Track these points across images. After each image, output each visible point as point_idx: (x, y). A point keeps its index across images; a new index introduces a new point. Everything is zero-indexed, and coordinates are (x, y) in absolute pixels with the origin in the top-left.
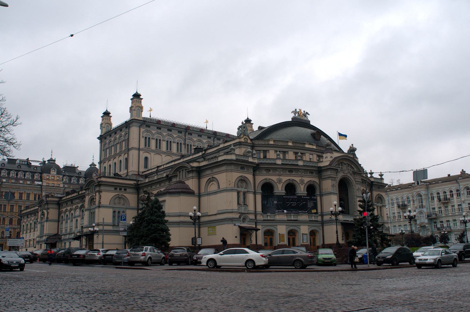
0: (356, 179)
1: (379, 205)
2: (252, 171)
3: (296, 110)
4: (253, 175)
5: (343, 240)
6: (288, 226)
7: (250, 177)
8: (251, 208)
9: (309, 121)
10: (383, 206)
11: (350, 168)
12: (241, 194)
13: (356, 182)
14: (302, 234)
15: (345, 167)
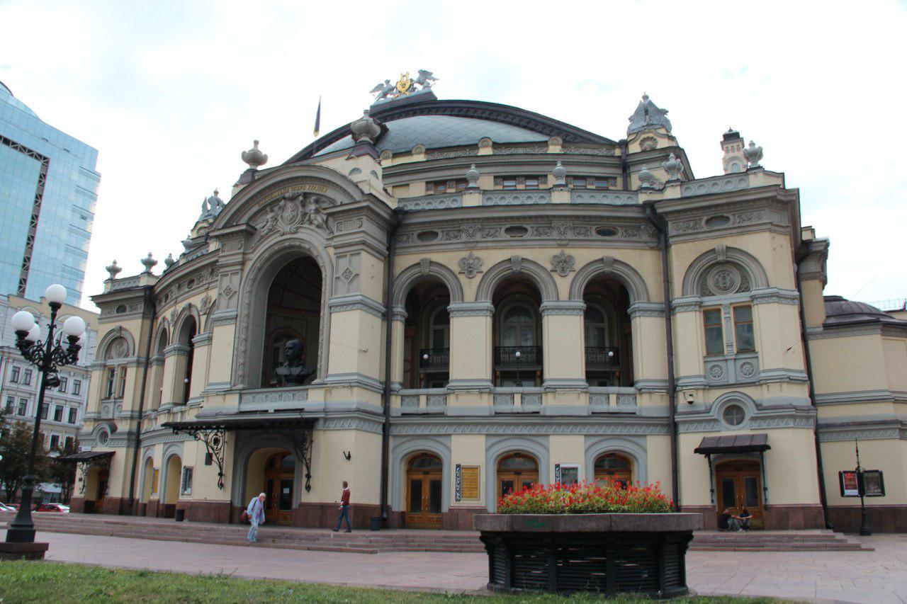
0: (335, 240)
1: (725, 300)
2: (141, 308)
3: (388, 82)
4: (143, 318)
5: (221, 485)
6: (166, 446)
7: (134, 325)
8: (128, 404)
9: (430, 93)
10: (753, 298)
11: (313, 207)
12: (118, 372)
13: (338, 251)
14: (185, 467)
15: (289, 210)
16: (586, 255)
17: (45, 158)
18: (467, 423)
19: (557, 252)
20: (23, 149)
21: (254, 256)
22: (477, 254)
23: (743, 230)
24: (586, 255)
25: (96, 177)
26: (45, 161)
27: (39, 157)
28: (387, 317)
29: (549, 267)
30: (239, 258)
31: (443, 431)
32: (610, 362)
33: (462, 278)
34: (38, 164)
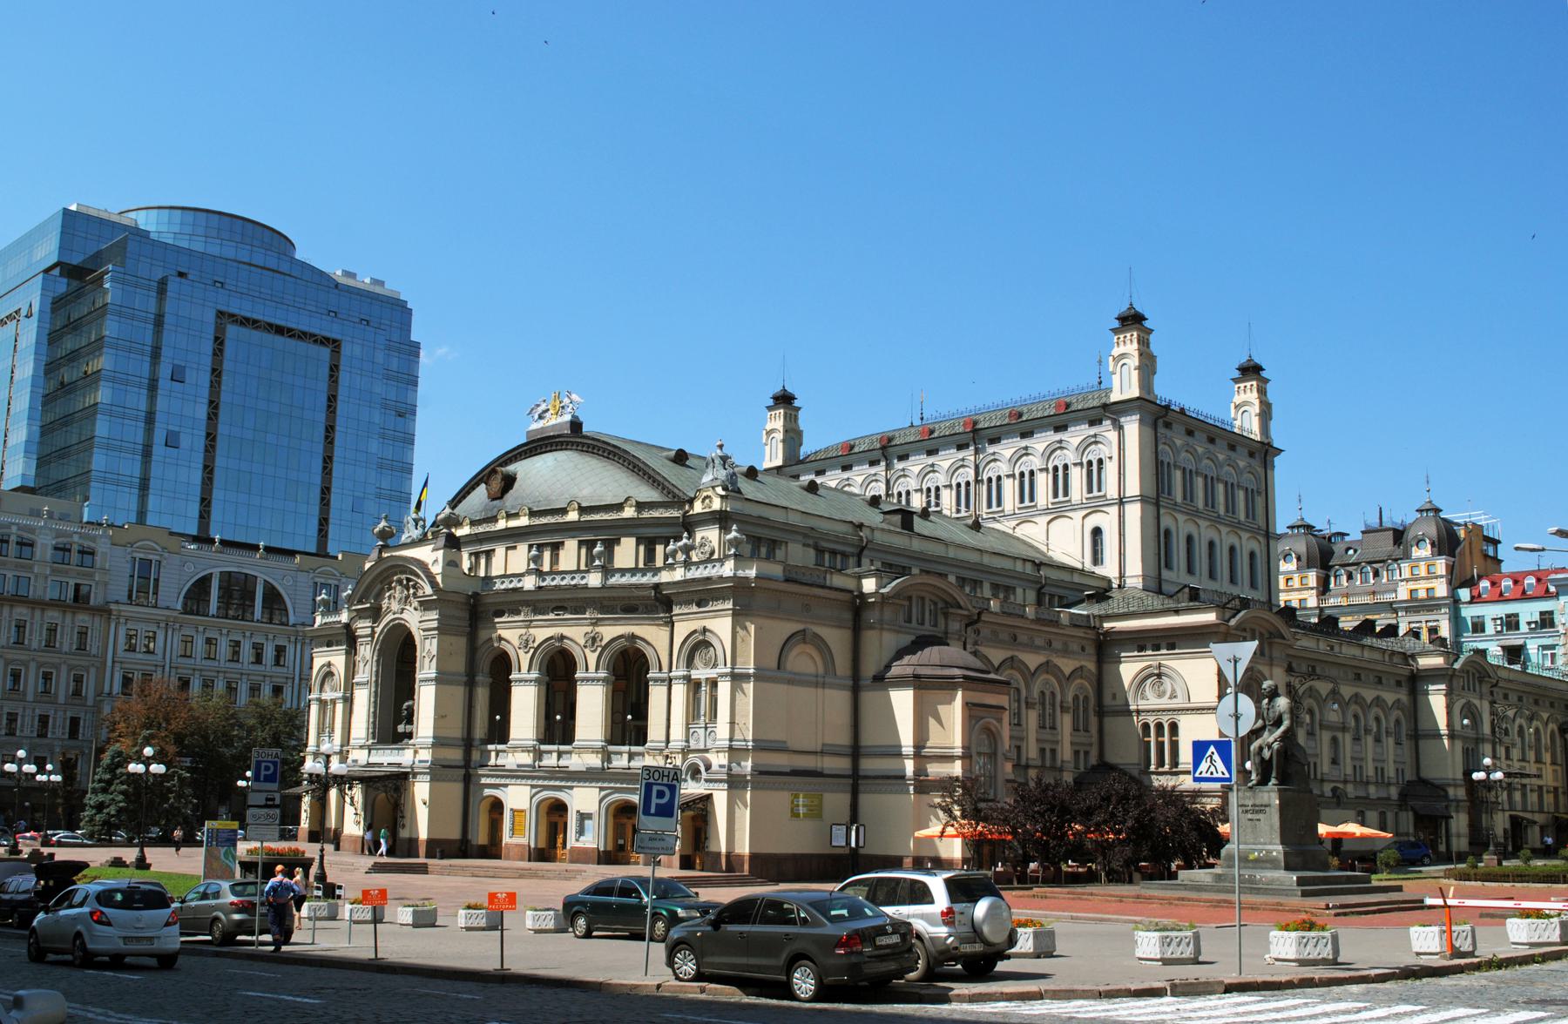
16: (609, 632)
17: (335, 341)
18: (518, 774)
19: (589, 629)
20: (303, 336)
21: (378, 630)
22: (532, 631)
23: (717, 614)
24: (609, 632)
25: (415, 349)
26: (334, 345)
27: (324, 341)
28: (471, 684)
29: (582, 642)
30: (369, 631)
31: (503, 781)
32: (628, 722)
33: (521, 652)
34: (325, 352)
